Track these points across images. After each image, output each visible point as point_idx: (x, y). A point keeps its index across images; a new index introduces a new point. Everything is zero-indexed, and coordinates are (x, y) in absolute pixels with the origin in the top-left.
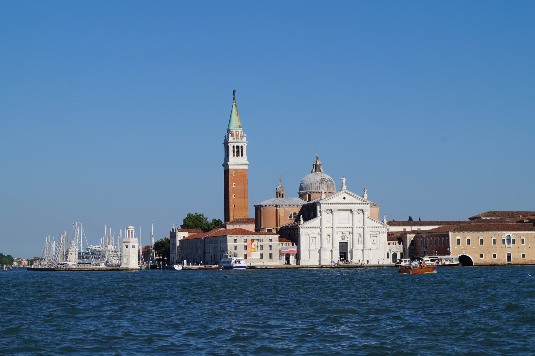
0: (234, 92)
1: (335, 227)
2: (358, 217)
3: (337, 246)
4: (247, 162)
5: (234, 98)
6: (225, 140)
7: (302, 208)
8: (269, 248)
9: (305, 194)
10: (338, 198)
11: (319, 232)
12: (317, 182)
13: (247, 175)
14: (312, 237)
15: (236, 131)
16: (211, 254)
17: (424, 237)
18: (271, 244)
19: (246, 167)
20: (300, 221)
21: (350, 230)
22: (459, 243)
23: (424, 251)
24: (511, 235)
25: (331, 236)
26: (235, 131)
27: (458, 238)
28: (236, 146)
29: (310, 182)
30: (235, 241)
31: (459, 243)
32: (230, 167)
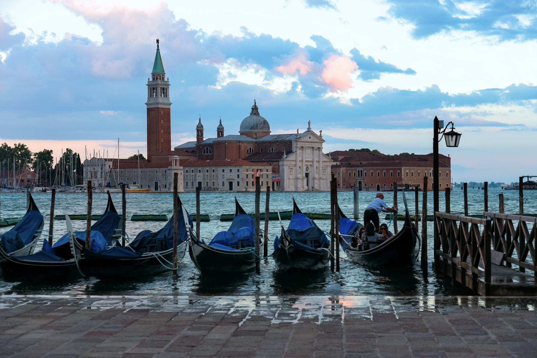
0: (158, 41)
1: (304, 160)
3: (305, 176)
5: (158, 45)
6: (149, 81)
11: (295, 164)
12: (261, 123)
15: (163, 75)
17: (359, 170)
20: (283, 154)
22: (407, 176)
23: (359, 181)
26: (162, 74)
27: (407, 171)
28: (163, 88)
29: (256, 123)
32: (160, 106)
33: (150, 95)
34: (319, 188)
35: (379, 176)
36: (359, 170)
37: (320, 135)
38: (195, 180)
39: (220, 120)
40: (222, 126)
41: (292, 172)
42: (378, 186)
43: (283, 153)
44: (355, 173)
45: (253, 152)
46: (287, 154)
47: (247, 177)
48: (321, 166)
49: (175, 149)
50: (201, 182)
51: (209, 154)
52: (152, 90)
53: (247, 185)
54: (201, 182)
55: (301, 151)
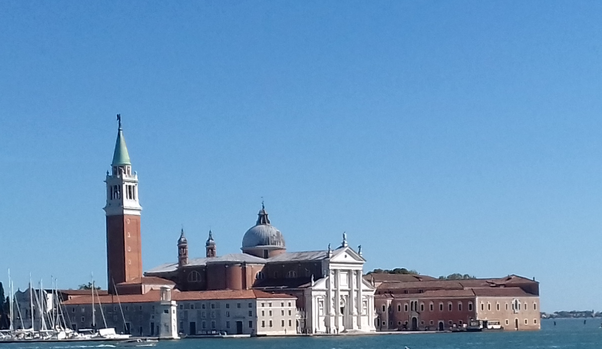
2: (354, 277)
4: (139, 207)
7: (265, 266)
8: (287, 313)
9: (261, 250)
10: (341, 257)
12: (274, 235)
13: (139, 222)
14: (320, 301)
15: (128, 167)
16: (190, 320)
18: (290, 308)
19: (138, 213)
20: (311, 282)
21: (347, 293)
22: (482, 309)
23: (413, 317)
24: (518, 300)
25: (335, 299)
30: (263, 305)
31: (482, 309)
32: (125, 212)
33: (110, 195)
34: (359, 328)
35: (441, 309)
36: (412, 302)
37: (359, 252)
38: (186, 319)
39: (210, 232)
40: (212, 240)
41: (323, 306)
42: (441, 323)
43: (311, 277)
44: (406, 306)
45: (263, 277)
46: (315, 280)
47: (263, 315)
48: (362, 297)
49: (146, 275)
50: (195, 323)
51: (196, 281)
52: (113, 188)
53: (263, 326)
54: (195, 323)
55: (333, 276)
